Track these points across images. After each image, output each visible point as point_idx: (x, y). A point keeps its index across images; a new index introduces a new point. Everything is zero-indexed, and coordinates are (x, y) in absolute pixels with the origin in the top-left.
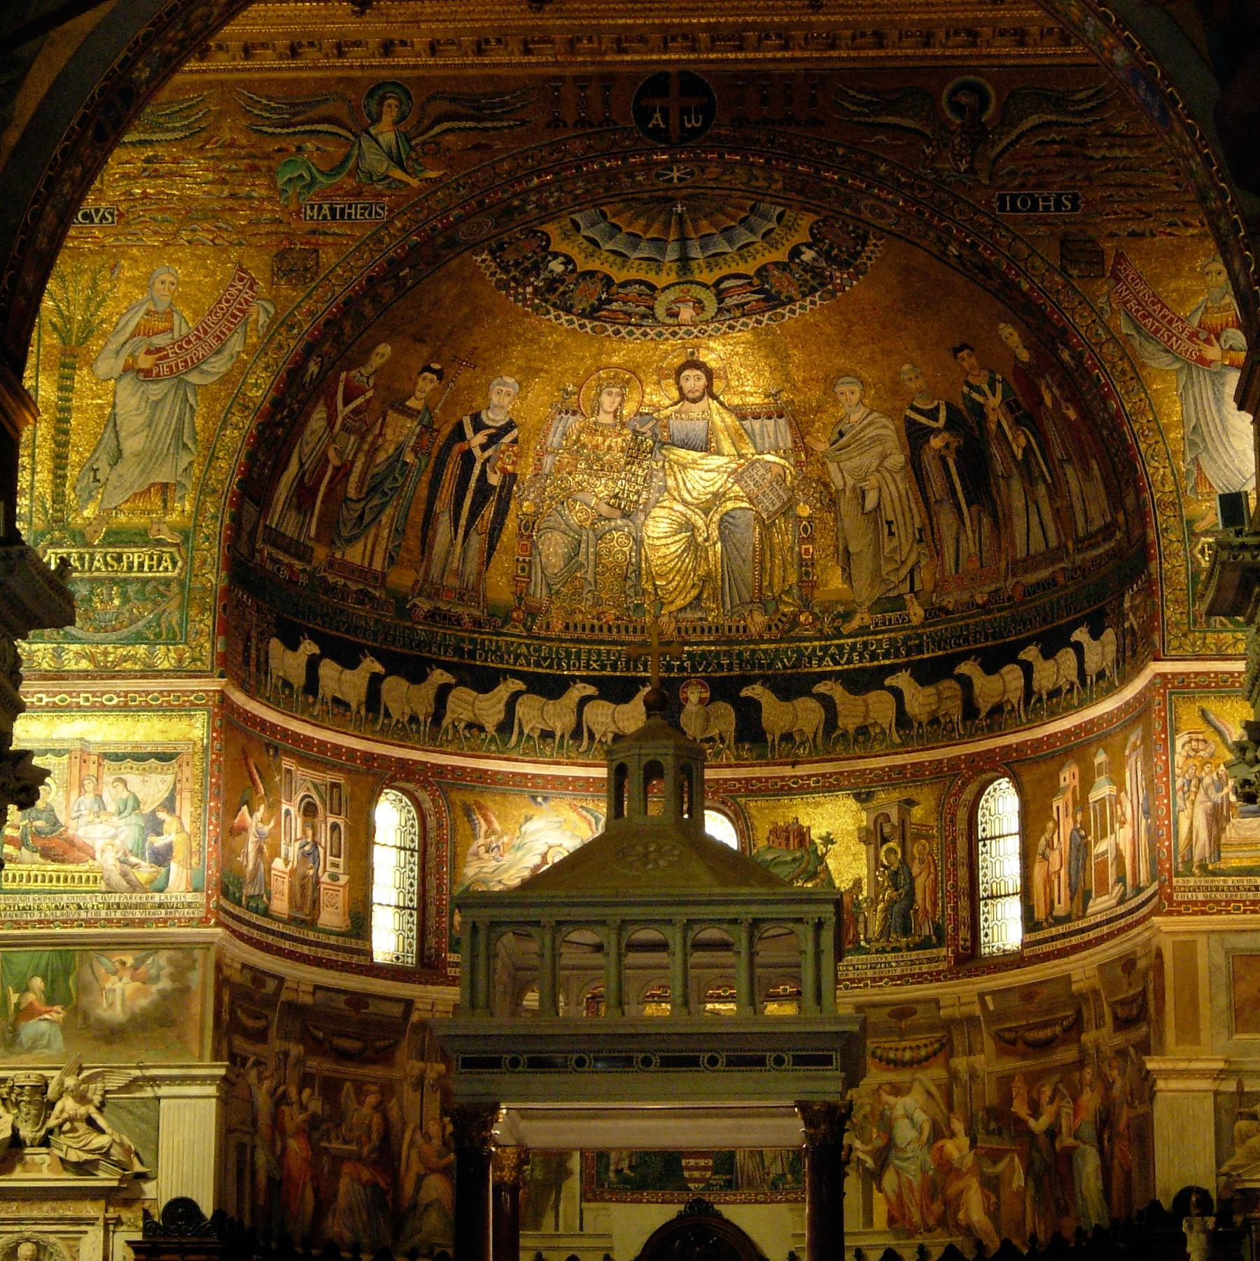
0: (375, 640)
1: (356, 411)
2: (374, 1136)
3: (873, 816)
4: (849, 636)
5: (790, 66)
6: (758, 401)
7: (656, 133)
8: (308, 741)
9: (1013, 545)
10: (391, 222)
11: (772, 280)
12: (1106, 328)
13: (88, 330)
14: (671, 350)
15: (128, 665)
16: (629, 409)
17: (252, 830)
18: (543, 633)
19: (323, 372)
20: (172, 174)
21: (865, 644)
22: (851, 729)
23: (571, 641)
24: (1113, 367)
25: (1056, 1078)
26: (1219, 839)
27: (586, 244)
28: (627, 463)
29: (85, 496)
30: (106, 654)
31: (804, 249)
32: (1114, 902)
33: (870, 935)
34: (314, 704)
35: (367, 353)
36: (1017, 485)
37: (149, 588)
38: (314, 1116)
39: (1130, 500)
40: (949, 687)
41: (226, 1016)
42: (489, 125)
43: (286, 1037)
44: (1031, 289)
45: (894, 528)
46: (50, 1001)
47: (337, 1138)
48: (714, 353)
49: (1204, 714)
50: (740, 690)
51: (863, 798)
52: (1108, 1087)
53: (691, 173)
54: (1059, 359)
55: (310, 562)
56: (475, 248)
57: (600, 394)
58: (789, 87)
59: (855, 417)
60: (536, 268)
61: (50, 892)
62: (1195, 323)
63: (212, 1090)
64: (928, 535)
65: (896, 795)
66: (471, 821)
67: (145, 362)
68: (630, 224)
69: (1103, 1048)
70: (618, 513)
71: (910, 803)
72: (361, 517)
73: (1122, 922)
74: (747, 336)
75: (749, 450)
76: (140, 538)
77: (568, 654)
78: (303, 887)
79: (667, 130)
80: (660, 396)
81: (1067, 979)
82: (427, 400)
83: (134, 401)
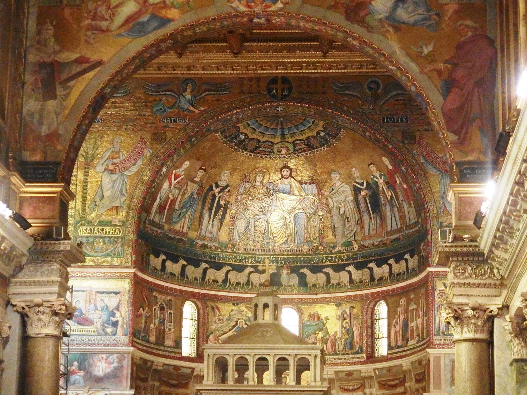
0: (184, 254)
1: (178, 182)
3: (341, 311)
4: (334, 254)
5: (317, 75)
6: (307, 179)
7: (274, 96)
8: (162, 286)
9: (386, 226)
10: (189, 124)
12: (416, 160)
13: (93, 157)
14: (279, 162)
15: (105, 264)
16: (266, 180)
17: (144, 315)
18: (237, 251)
20: (120, 107)
21: (340, 256)
22: (335, 283)
23: (247, 254)
27: (251, 130)
28: (265, 198)
29: (92, 210)
30: (98, 260)
32: (416, 342)
33: (340, 349)
36: (388, 207)
37: (112, 239)
39: (423, 215)
40: (366, 271)
41: (134, 374)
42: (220, 93)
43: (154, 380)
45: (349, 220)
46: (80, 369)
48: (292, 164)
50: (299, 270)
51: (338, 305)
53: (285, 109)
54: (401, 169)
56: (216, 131)
57: (256, 176)
58: (316, 81)
60: (236, 137)
61: (80, 335)
64: (360, 222)
65: (349, 305)
66: (214, 311)
67: (111, 167)
68: (266, 124)
70: (262, 213)
71: (353, 307)
72: (180, 214)
73: (418, 349)
74: (303, 158)
75: (303, 194)
76: (109, 223)
77: (245, 258)
78: (160, 332)
79: (277, 95)
80: (275, 177)
81: (401, 366)
83: (108, 180)
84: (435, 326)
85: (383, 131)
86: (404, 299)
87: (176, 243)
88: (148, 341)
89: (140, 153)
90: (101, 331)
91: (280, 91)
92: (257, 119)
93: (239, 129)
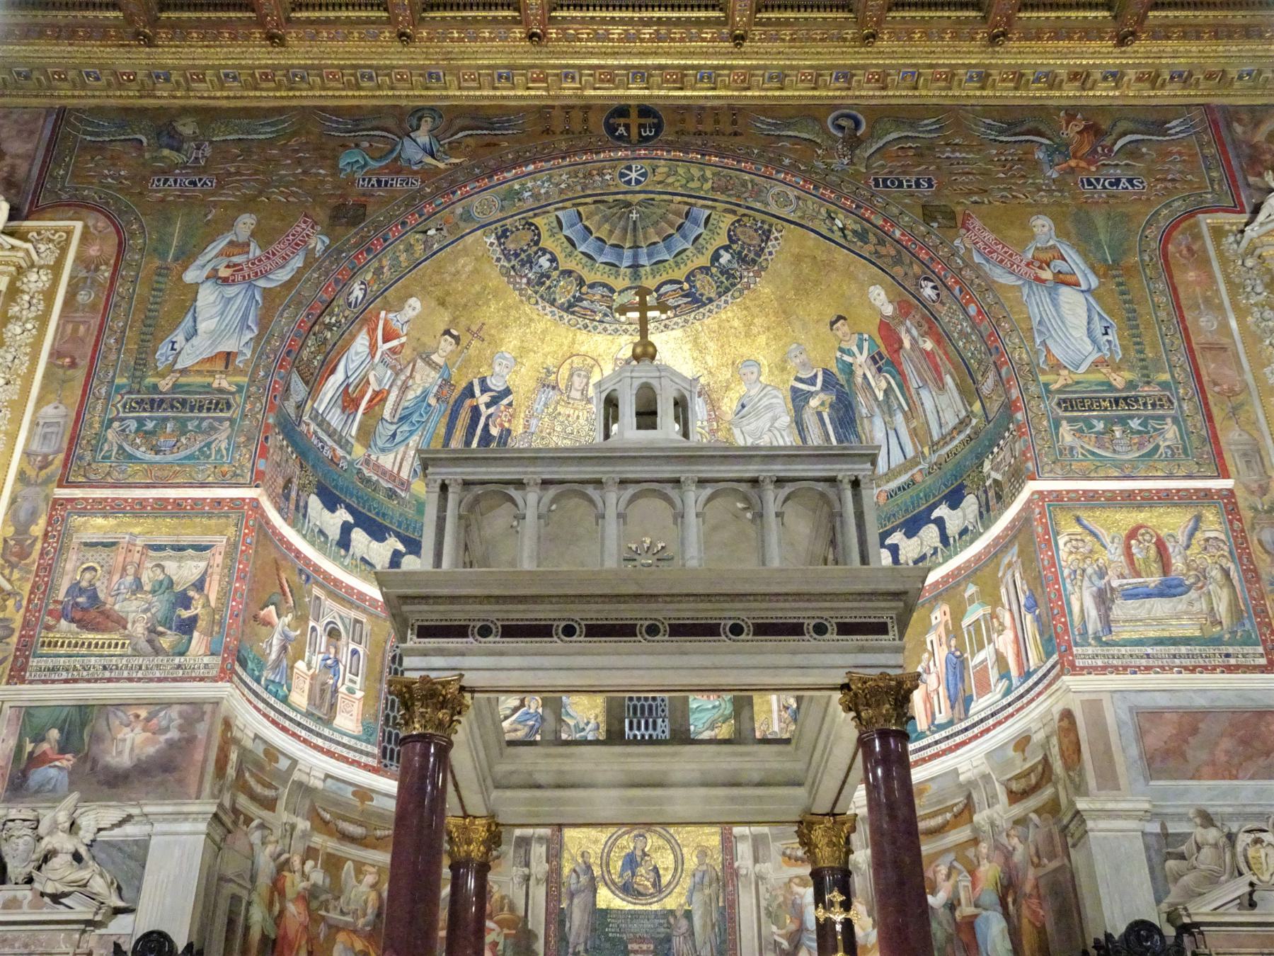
1: (393, 351)
2: (369, 911)
5: (716, 103)
8: (337, 582)
10: (423, 189)
11: (698, 284)
12: (961, 258)
17: (279, 629)
19: (368, 301)
24: (972, 283)
25: (951, 856)
26: (1108, 616)
27: (566, 244)
31: (722, 252)
32: (999, 696)
34: (345, 557)
35: (403, 300)
36: (878, 422)
38: (315, 885)
39: (988, 385)
44: (903, 235)
46: (63, 750)
47: (335, 907)
49: (1078, 520)
52: (1008, 855)
53: (644, 175)
55: (350, 454)
59: (753, 392)
60: (530, 262)
62: (1030, 256)
63: (203, 827)
67: (224, 273)
68: (598, 229)
69: (997, 823)
72: (394, 435)
78: (323, 691)
81: (955, 772)
82: (447, 358)
83: (212, 298)
84: (1072, 620)
85: (879, 202)
86: (946, 608)
87: (381, 496)
88: (285, 700)
89: (297, 244)
90: (143, 645)
91: (634, 130)
92: (581, 209)
93: (539, 235)
